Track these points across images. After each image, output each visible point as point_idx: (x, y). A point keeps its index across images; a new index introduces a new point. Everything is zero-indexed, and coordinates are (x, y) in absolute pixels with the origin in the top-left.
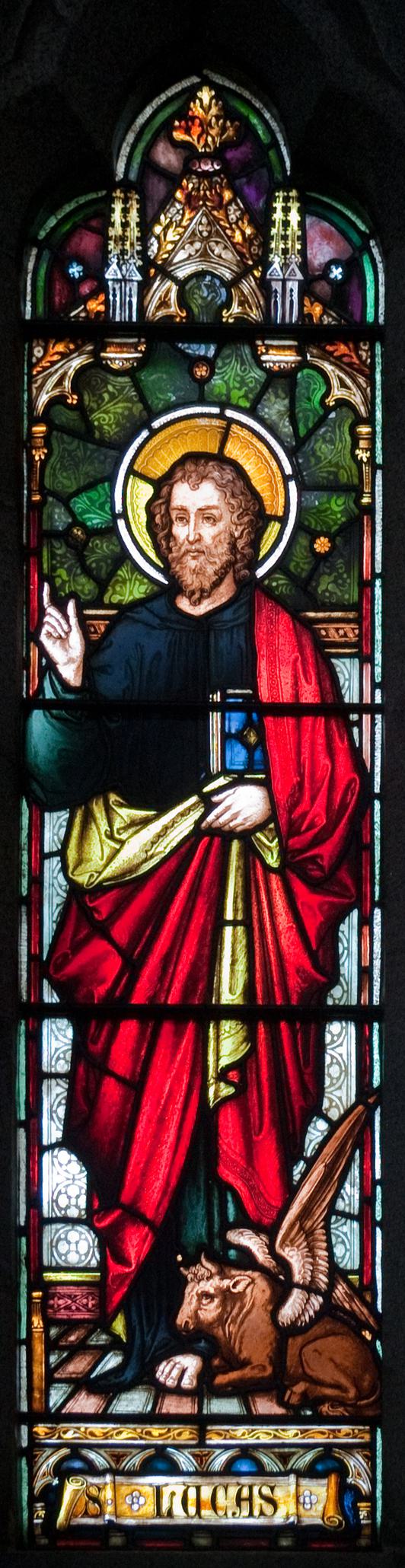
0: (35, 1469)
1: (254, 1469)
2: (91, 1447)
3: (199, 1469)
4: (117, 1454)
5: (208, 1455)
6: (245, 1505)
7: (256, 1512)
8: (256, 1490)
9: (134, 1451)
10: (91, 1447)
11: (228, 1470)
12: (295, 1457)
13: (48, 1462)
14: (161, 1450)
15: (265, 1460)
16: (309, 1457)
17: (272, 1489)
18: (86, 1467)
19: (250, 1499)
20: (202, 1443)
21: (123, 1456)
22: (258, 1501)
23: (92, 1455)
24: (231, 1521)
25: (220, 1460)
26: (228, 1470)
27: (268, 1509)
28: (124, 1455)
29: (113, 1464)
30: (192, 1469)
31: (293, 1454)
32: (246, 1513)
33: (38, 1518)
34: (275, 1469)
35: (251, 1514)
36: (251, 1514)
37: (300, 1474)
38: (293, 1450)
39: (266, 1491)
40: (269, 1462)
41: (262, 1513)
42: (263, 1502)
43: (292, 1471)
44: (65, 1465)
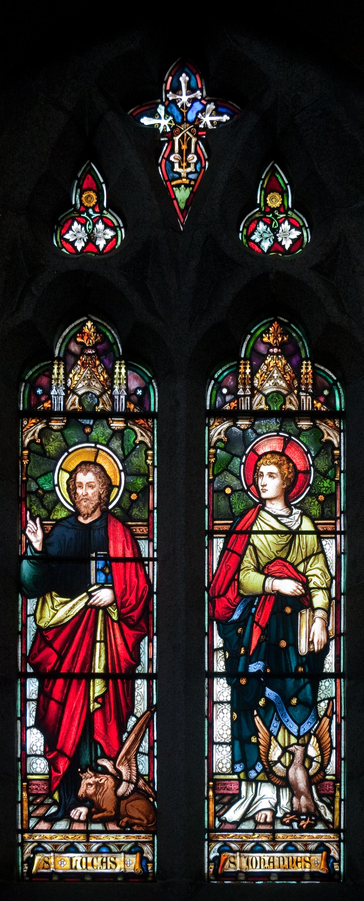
0: (24, 851)
1: (108, 851)
2: (45, 842)
3: (87, 851)
4: (56, 845)
5: (90, 845)
6: (104, 865)
7: (109, 867)
8: (108, 859)
9: (62, 844)
10: (45, 842)
11: (98, 851)
12: (124, 846)
13: (29, 848)
14: (72, 844)
15: (112, 847)
16: (129, 846)
17: (115, 858)
18: (44, 850)
19: (106, 862)
20: (88, 841)
21: (58, 846)
22: (109, 863)
23: (46, 846)
24: (99, 871)
25: (95, 848)
26: (98, 851)
27: (113, 866)
28: (58, 845)
29: (54, 849)
30: (84, 851)
31: (123, 845)
32: (105, 868)
33: (25, 869)
34: (116, 851)
35: (107, 868)
36: (107, 868)
37: (125, 853)
38: (123, 843)
39: (112, 859)
40: (113, 848)
41: (111, 868)
42: (111, 863)
43: (122, 852)
44: (36, 849)
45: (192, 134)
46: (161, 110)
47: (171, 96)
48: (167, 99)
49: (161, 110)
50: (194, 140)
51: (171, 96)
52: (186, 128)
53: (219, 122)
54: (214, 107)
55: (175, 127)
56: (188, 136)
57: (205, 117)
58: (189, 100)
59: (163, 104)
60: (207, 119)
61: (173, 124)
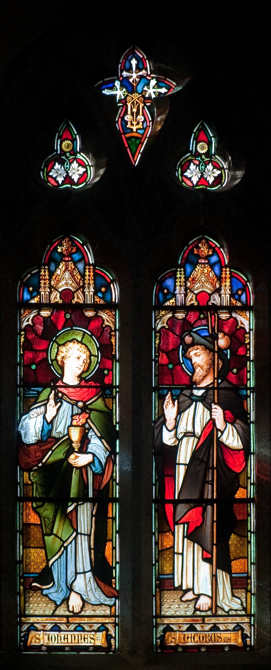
45: (141, 102)
46: (117, 84)
47: (125, 74)
48: (122, 76)
49: (117, 84)
50: (141, 105)
51: (125, 74)
52: (136, 97)
53: (160, 93)
54: (156, 82)
55: (127, 96)
56: (137, 102)
57: (149, 89)
58: (137, 77)
59: (118, 79)
60: (151, 91)
61: (126, 94)
